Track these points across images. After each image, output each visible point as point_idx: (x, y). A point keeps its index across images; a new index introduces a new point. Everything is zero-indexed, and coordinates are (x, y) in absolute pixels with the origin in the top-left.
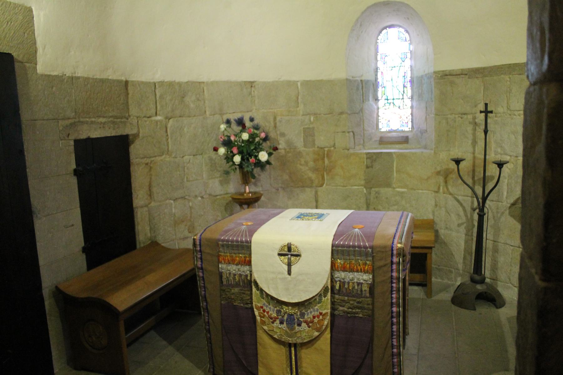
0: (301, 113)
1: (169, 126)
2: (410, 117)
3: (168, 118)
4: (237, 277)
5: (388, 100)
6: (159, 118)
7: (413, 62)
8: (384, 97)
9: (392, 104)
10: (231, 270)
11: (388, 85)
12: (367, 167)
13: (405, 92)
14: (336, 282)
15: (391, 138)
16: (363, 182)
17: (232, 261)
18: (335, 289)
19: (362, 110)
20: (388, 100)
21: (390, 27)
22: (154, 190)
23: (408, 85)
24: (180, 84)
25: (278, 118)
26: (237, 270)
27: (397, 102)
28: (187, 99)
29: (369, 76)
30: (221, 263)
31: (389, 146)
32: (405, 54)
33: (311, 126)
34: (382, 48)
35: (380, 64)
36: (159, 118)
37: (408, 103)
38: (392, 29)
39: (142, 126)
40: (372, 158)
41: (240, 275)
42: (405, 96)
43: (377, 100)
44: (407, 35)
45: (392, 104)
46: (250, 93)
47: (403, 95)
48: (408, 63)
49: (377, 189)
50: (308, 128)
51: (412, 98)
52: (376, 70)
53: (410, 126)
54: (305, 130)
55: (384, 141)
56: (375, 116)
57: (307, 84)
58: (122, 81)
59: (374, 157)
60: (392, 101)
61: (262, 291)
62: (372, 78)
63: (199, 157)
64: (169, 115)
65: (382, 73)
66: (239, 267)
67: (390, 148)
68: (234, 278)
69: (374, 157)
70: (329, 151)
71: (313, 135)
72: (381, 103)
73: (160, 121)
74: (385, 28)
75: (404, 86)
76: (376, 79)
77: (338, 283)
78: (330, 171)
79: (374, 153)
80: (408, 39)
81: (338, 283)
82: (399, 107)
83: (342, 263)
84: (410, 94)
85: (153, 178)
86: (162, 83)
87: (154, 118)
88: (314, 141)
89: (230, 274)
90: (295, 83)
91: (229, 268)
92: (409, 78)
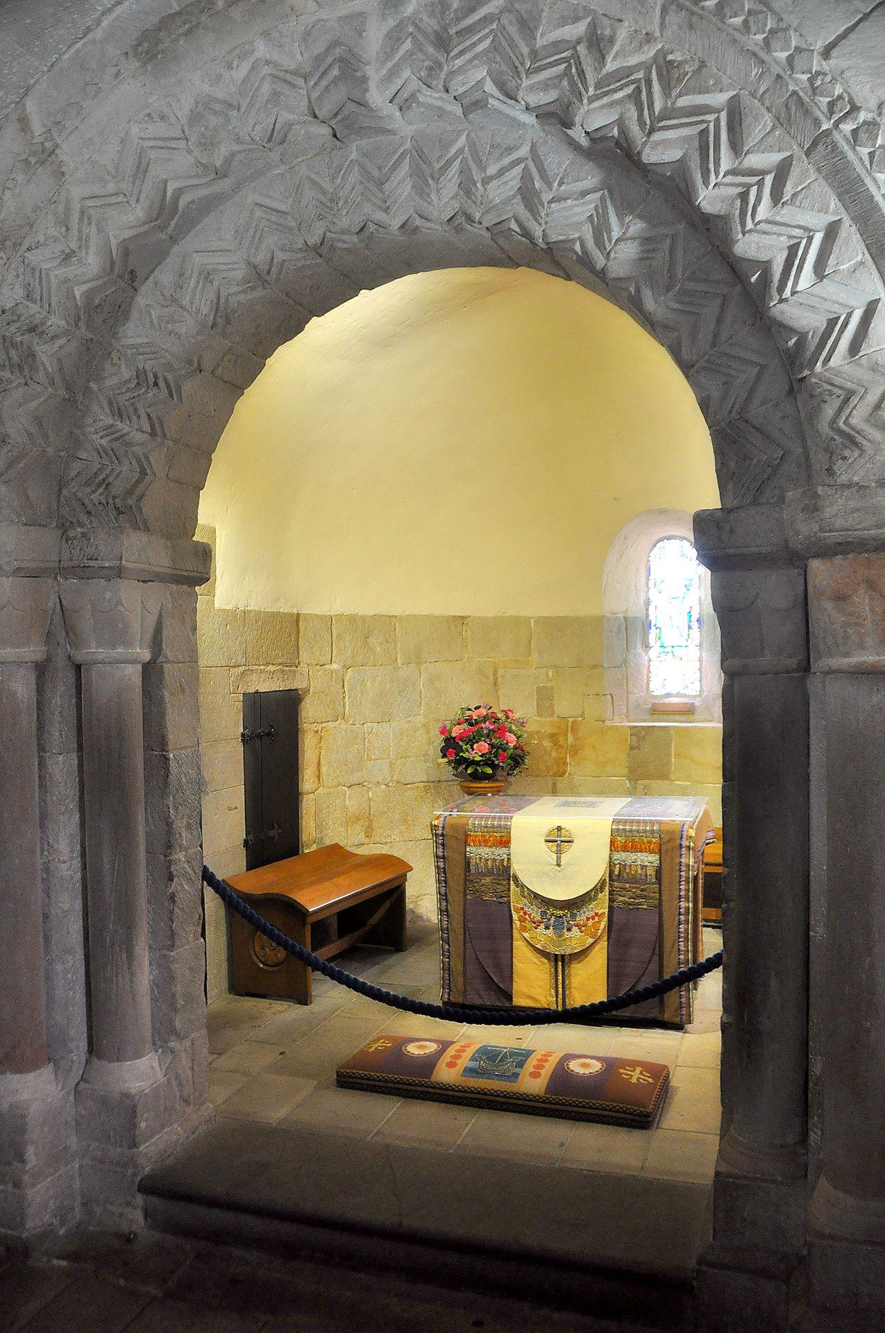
0: (535, 665)
1: (347, 678)
3: (346, 668)
6: (334, 666)
8: (659, 644)
12: (632, 748)
15: (669, 704)
16: (625, 771)
19: (625, 662)
21: (669, 538)
22: (324, 769)
23: (695, 625)
24: (363, 618)
25: (500, 672)
27: (678, 651)
28: (372, 640)
29: (635, 611)
31: (666, 717)
33: (549, 685)
35: (653, 594)
36: (334, 666)
37: (694, 652)
39: (315, 678)
40: (640, 735)
43: (647, 647)
46: (460, 634)
49: (646, 782)
50: (546, 688)
51: (701, 646)
52: (648, 603)
53: (697, 686)
54: (539, 690)
55: (657, 710)
56: (645, 671)
57: (541, 621)
58: (291, 615)
59: (643, 733)
60: (670, 649)
62: (642, 615)
63: (386, 725)
64: (348, 663)
67: (668, 721)
69: (643, 733)
70: (574, 723)
71: (551, 698)
73: (337, 671)
74: (661, 540)
75: (690, 627)
76: (647, 616)
78: (576, 753)
79: (642, 727)
84: (697, 641)
85: (323, 751)
86: (340, 617)
87: (327, 667)
88: (552, 706)
90: (526, 620)
92: (695, 616)
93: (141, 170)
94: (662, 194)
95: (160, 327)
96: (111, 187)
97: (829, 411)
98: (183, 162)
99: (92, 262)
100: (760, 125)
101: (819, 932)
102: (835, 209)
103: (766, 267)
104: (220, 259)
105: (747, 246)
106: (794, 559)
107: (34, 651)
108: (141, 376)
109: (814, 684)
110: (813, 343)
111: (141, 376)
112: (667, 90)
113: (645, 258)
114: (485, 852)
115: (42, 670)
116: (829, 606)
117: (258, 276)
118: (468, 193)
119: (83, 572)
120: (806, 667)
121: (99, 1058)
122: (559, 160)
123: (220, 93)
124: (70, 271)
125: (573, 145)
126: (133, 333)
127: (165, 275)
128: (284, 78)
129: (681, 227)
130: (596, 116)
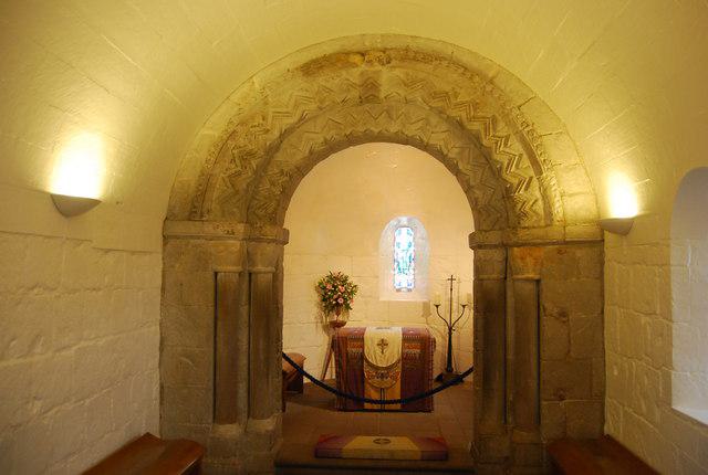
11: (401, 261)
48: (412, 248)
61: (368, 362)
93: (296, 106)
94: (475, 140)
95: (290, 156)
96: (285, 110)
97: (519, 206)
98: (313, 106)
99: (276, 134)
100: (501, 125)
101: (510, 357)
102: (521, 150)
103: (502, 164)
104: (315, 136)
105: (497, 157)
106: (505, 246)
107: (240, 268)
108: (282, 172)
109: (509, 283)
110: (515, 186)
111: (282, 172)
112: (475, 110)
113: (460, 153)
114: (354, 350)
115: (240, 274)
116: (519, 261)
117: (326, 141)
118: (404, 126)
119: (259, 240)
120: (506, 278)
121: (254, 418)
122: (434, 120)
123: (328, 85)
124: (269, 136)
125: (441, 117)
126: (279, 157)
127: (293, 139)
128: (353, 85)
129: (472, 146)
130: (454, 113)
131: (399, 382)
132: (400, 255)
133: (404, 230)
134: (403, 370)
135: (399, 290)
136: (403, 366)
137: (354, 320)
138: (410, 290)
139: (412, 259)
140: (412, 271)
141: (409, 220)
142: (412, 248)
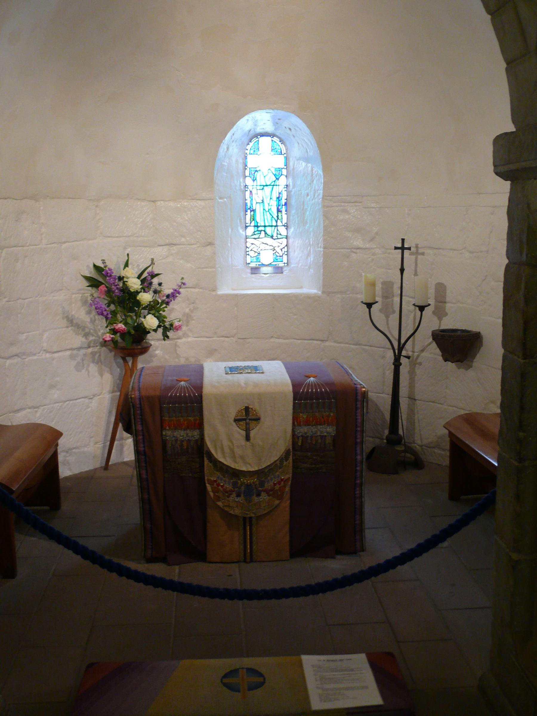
2: (286, 249)
4: (185, 444)
5: (258, 227)
7: (290, 180)
8: (253, 224)
9: (263, 233)
10: (179, 436)
11: (259, 209)
13: (280, 217)
14: (298, 438)
17: (178, 426)
18: (299, 447)
20: (258, 227)
26: (185, 435)
27: (269, 230)
30: (165, 429)
32: (280, 169)
34: (252, 162)
35: (249, 181)
38: (262, 139)
41: (189, 441)
42: (279, 223)
44: (282, 147)
45: (263, 233)
47: (277, 222)
48: (283, 181)
53: (285, 261)
60: (263, 228)
65: (251, 192)
66: (188, 431)
68: (182, 445)
72: (250, 230)
75: (279, 211)
77: (300, 438)
80: (284, 151)
81: (300, 438)
82: (272, 237)
83: (305, 417)
84: (285, 221)
89: (176, 440)
91: (175, 434)
92: (283, 202)
131: (286, 504)
132: (258, 196)
133: (265, 141)
134: (294, 474)
135: (255, 270)
136: (295, 467)
137: (162, 356)
138: (278, 270)
139: (285, 205)
140: (283, 231)
141: (276, 123)
142: (283, 181)
